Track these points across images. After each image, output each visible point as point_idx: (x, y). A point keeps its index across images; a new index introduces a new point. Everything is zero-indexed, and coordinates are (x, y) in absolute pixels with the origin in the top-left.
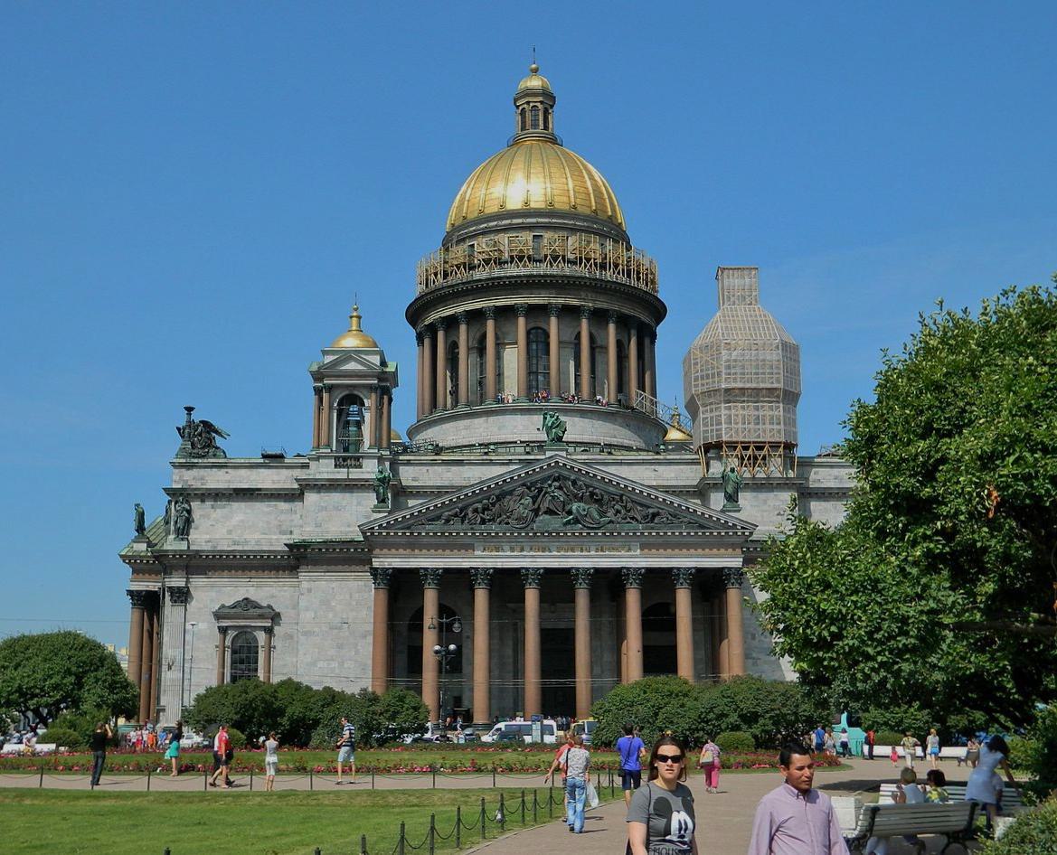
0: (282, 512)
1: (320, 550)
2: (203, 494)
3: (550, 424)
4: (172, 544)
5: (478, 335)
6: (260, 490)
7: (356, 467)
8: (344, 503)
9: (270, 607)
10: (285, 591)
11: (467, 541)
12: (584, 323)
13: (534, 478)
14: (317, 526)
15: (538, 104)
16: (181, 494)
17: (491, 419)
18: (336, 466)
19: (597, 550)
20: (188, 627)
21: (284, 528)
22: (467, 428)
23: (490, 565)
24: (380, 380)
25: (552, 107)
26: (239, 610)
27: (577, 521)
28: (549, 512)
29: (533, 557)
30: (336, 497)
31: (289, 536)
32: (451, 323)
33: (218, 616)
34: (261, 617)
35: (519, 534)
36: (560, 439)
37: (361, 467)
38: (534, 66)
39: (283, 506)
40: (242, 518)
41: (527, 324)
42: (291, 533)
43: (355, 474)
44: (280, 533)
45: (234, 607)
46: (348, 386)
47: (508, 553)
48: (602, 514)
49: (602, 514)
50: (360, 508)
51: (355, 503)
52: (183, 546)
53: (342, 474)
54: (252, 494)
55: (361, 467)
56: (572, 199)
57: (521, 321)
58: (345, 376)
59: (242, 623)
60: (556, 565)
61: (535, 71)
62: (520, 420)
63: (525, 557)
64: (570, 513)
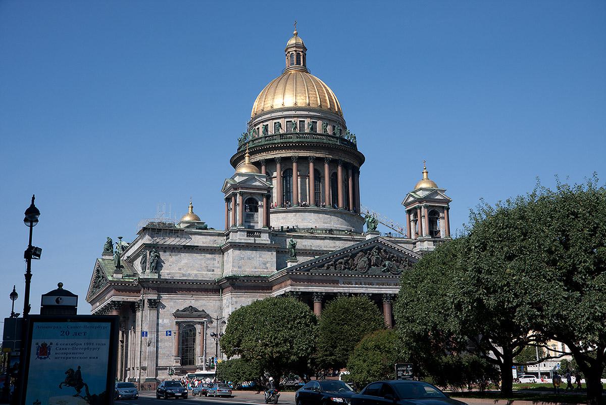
0: (208, 259)
1: (244, 280)
2: (166, 248)
3: (370, 221)
4: (149, 275)
5: (283, 170)
6: (198, 246)
7: (257, 236)
8: (253, 256)
9: (203, 311)
10: (211, 302)
11: (336, 278)
12: (340, 169)
13: (366, 248)
14: (239, 267)
15: (300, 53)
16: (154, 247)
17: (298, 214)
18: (247, 236)
19: (394, 285)
20: (160, 321)
21: (209, 268)
22: (283, 218)
23: (346, 291)
24: (269, 192)
25: (305, 54)
26: (188, 313)
27: (388, 271)
28: (374, 265)
29: (366, 287)
30: (248, 253)
31: (213, 273)
32: (270, 163)
33: (177, 315)
34: (199, 317)
35: (362, 276)
36: (375, 228)
37: (260, 237)
38: (295, 32)
39: (209, 256)
40: (186, 262)
41: (314, 166)
42: (213, 271)
43: (258, 241)
44: (207, 271)
45: (184, 310)
46: (251, 193)
47: (354, 285)
48: (398, 267)
49: (398, 267)
50: (261, 259)
51: (258, 256)
52: (156, 276)
53: (251, 240)
54: (193, 249)
55: (260, 237)
56: (319, 102)
57: (311, 165)
58: (250, 188)
59: (189, 320)
60: (376, 292)
61: (296, 34)
62: (313, 216)
63: (363, 287)
64: (384, 266)
